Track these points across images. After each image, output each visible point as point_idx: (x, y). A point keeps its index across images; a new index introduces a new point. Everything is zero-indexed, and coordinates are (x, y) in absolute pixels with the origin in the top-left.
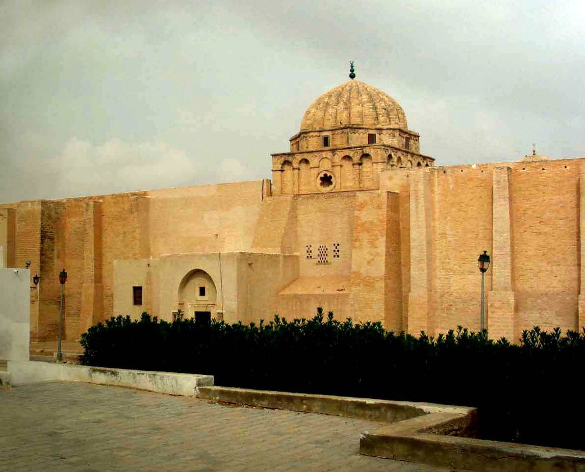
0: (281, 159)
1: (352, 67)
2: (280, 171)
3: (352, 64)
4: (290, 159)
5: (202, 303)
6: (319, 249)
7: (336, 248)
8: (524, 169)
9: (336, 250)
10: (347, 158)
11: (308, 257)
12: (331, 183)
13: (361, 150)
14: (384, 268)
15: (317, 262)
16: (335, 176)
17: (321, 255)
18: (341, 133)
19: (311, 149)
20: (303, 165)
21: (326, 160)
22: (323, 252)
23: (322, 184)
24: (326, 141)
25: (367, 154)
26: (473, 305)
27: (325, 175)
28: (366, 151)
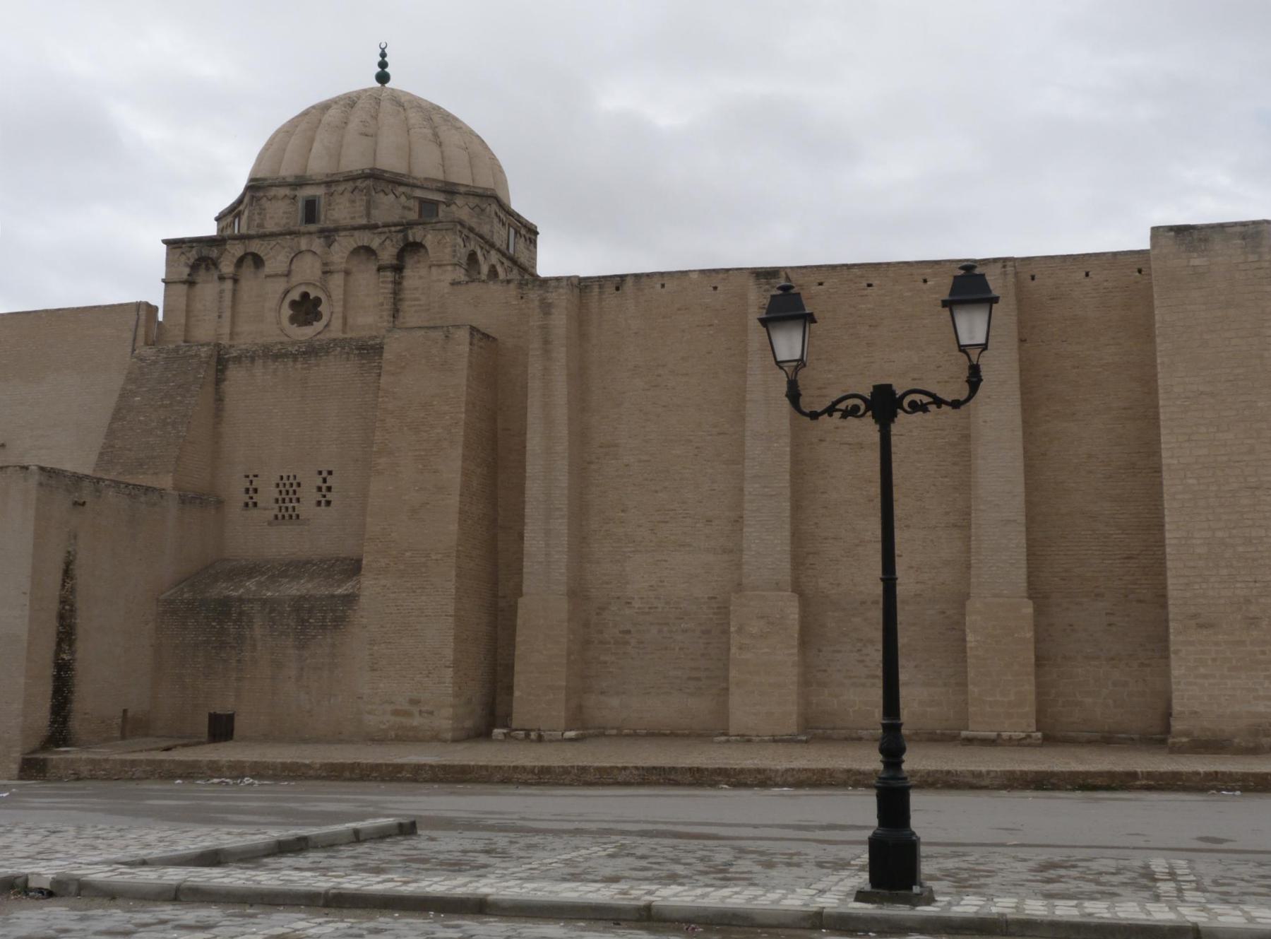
0: (189, 255)
1: (383, 55)
2: (184, 282)
3: (383, 50)
4: (214, 253)
7: (325, 481)
8: (821, 284)
9: (324, 487)
10: (367, 252)
11: (247, 505)
12: (318, 316)
13: (400, 235)
14: (454, 527)
15: (272, 518)
16: (329, 297)
18: (350, 189)
19: (270, 227)
20: (247, 270)
21: (308, 258)
22: (289, 490)
23: (293, 320)
26: (685, 631)
27: (305, 296)
28: (416, 234)
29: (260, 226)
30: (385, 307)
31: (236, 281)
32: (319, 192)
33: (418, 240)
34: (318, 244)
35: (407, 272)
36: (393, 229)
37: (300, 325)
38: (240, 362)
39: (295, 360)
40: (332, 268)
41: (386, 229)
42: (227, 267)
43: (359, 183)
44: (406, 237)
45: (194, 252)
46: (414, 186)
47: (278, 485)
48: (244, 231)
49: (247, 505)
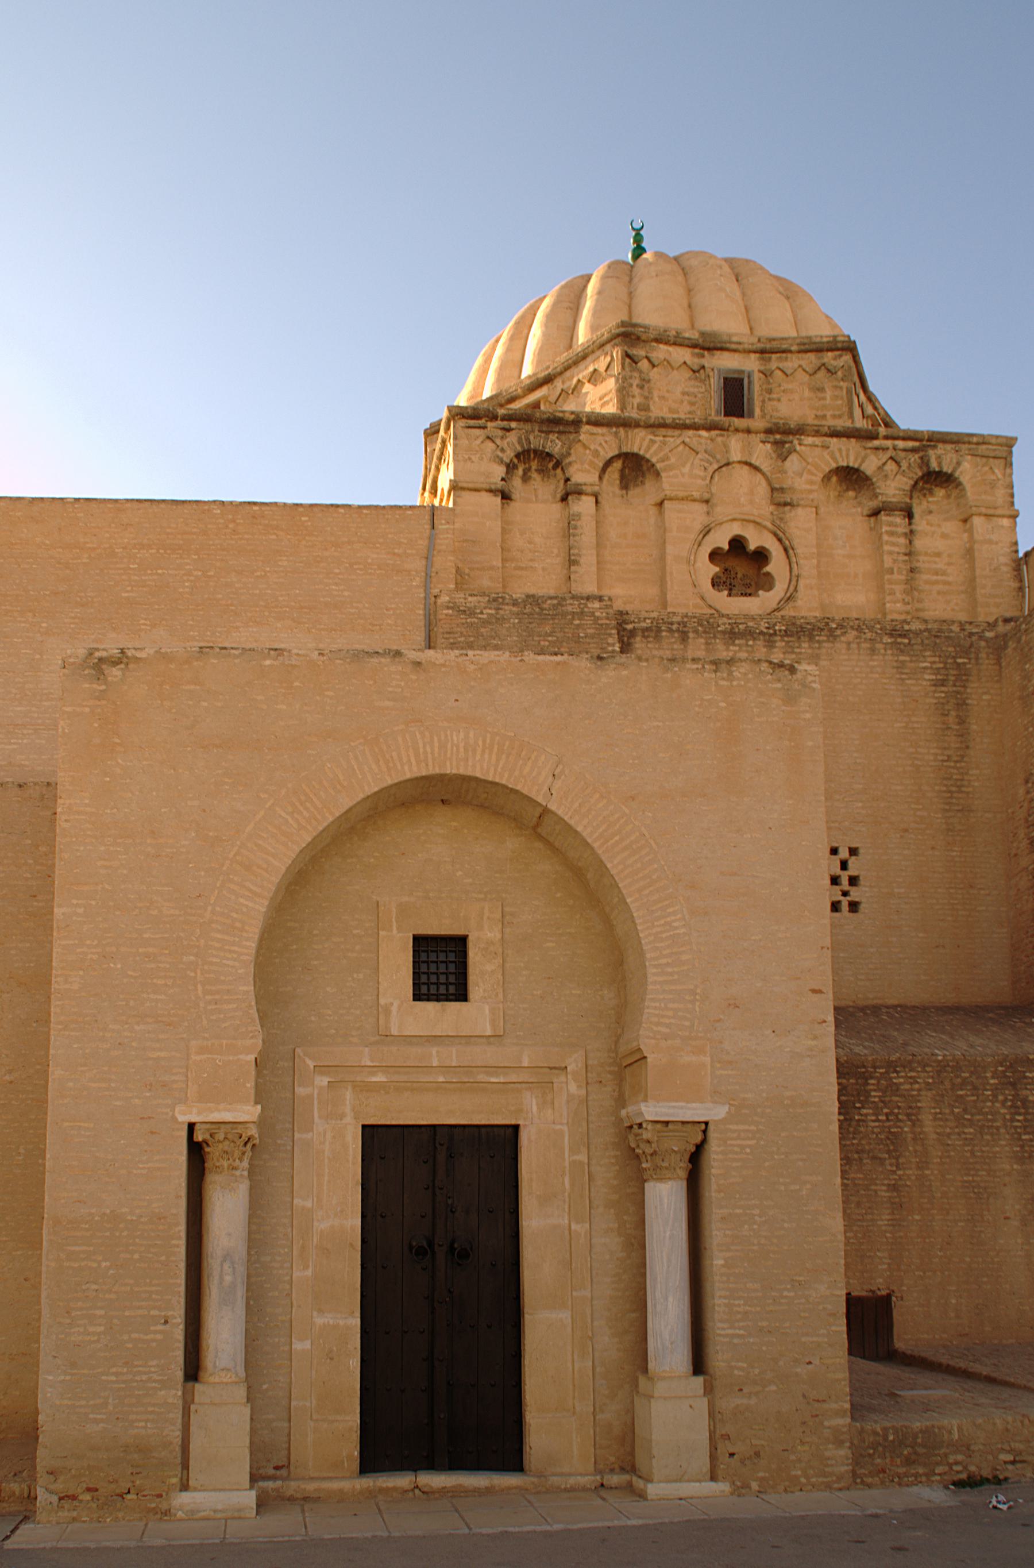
4: (555, 445)
5: (435, 1056)
10: (850, 478)
24: (735, 397)
27: (737, 544)
29: (644, 408)
32: (751, 364)
33: (947, 469)
35: (920, 523)
36: (900, 444)
38: (658, 637)
40: (795, 498)
41: (889, 443)
43: (828, 357)
44: (924, 462)
45: (512, 437)
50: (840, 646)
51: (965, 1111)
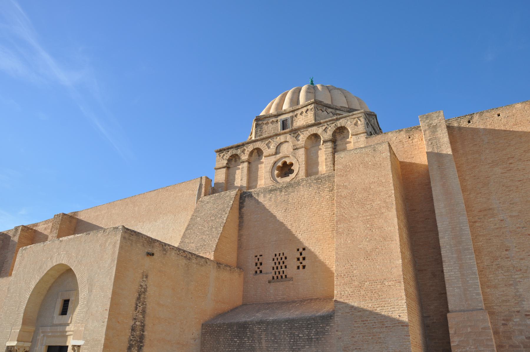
2: (224, 167)
6: (274, 260)
7: (301, 254)
11: (256, 272)
12: (292, 172)
17: (277, 268)
25: (341, 127)
27: (285, 163)
30: (328, 160)
31: (249, 163)
34: (288, 137)
37: (282, 177)
39: (281, 191)
42: (245, 157)
46: (336, 109)
47: (274, 260)
48: (253, 138)
49: (256, 272)
50: (301, 187)
51: (275, 339)
